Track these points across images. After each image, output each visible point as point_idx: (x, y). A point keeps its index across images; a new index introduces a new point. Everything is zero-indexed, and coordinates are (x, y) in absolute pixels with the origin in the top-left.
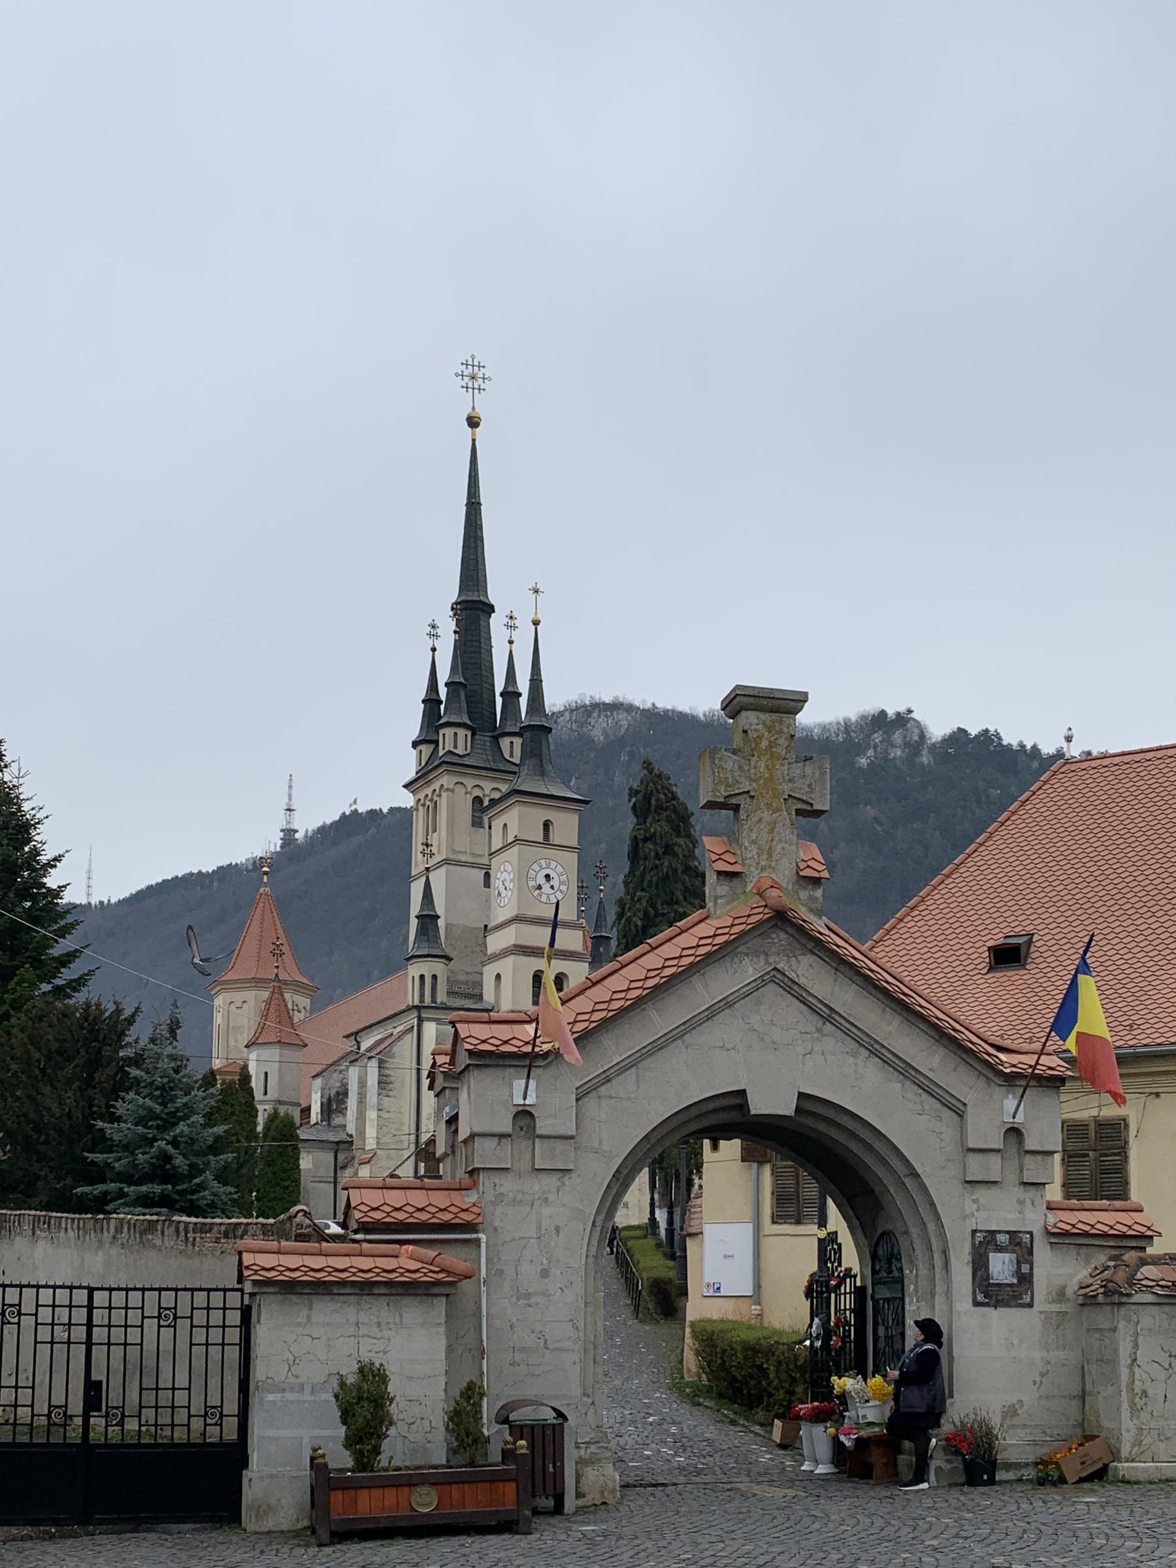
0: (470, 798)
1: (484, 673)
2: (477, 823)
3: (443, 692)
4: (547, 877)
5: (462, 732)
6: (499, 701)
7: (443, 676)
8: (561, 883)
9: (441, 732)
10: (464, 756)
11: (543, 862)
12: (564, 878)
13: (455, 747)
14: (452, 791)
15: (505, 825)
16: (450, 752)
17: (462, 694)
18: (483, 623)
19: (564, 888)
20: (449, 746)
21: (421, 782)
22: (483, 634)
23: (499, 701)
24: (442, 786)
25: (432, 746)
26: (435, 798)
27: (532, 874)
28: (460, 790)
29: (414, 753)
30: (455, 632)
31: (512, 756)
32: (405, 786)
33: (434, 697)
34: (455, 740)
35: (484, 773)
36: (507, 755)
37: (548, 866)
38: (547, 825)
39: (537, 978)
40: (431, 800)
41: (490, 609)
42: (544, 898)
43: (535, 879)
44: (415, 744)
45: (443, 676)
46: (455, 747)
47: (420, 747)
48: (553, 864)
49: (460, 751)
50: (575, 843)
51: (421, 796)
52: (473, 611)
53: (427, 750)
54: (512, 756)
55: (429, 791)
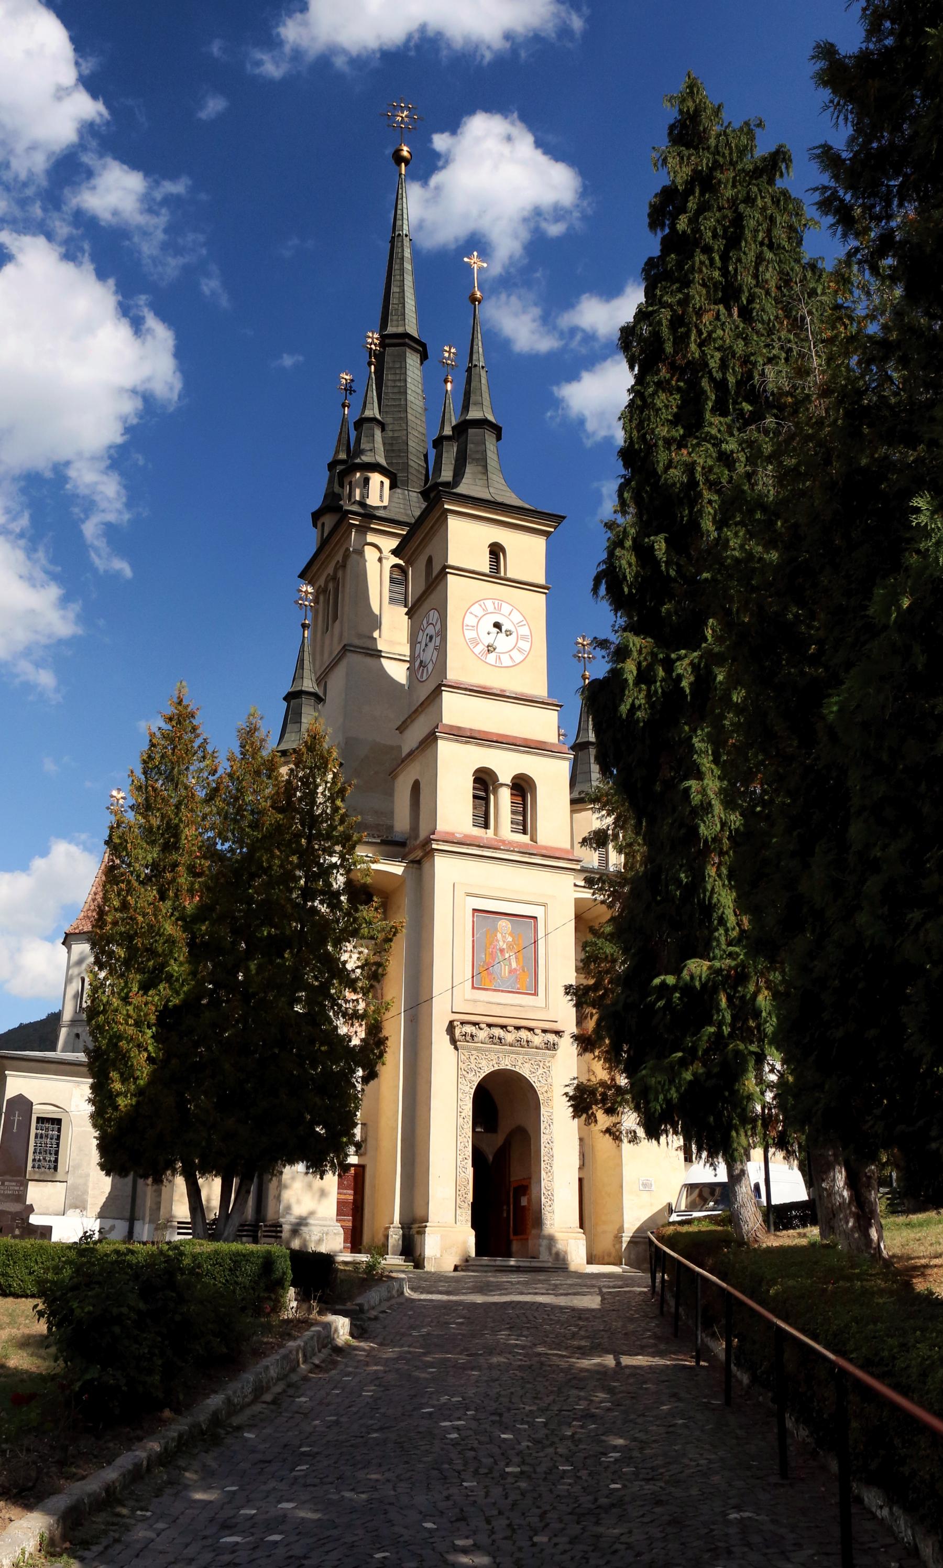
1: (410, 416)
4: (497, 625)
5: (376, 479)
10: (377, 508)
11: (489, 604)
15: (430, 561)
17: (378, 433)
18: (409, 361)
19: (525, 645)
21: (322, 557)
26: (340, 574)
27: (470, 620)
38: (496, 551)
39: (484, 781)
44: (316, 516)
47: (319, 525)
48: (506, 608)
50: (542, 580)
51: (321, 582)
53: (329, 521)
55: (330, 570)
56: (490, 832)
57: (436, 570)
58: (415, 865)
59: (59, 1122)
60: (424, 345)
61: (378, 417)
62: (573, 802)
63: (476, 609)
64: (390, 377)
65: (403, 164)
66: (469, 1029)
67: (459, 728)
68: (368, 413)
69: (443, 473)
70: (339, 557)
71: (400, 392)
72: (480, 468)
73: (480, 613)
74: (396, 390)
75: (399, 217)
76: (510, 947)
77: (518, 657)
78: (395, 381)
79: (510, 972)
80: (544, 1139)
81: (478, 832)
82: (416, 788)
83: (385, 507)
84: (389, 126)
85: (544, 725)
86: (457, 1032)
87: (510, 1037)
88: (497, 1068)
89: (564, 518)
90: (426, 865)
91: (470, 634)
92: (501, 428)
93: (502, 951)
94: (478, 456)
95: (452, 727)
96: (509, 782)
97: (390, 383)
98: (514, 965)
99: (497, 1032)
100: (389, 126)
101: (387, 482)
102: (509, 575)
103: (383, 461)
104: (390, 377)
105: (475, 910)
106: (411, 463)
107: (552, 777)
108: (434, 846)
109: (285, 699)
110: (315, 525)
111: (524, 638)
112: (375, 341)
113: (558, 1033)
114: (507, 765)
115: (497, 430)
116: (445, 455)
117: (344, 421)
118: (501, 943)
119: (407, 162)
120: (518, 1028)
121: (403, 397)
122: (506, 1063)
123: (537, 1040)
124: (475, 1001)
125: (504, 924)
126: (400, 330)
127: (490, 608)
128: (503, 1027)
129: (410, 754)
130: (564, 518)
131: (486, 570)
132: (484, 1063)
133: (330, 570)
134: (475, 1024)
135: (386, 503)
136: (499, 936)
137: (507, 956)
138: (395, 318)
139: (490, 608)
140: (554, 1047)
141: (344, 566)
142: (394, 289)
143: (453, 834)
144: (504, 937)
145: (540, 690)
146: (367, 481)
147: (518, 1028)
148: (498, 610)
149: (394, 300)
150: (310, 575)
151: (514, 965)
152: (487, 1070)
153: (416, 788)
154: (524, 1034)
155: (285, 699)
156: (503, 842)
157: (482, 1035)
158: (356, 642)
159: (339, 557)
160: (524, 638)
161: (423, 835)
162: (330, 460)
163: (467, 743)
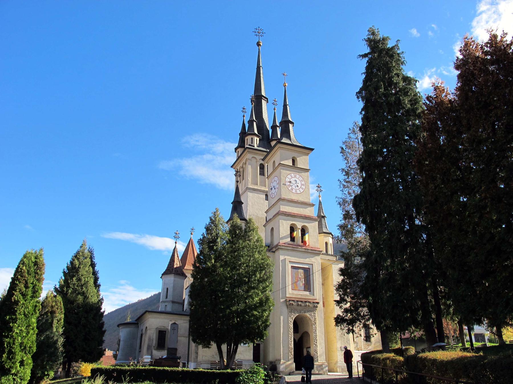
0: (259, 164)
3: (247, 126)
8: (302, 185)
12: (303, 183)
13: (252, 143)
14: (251, 160)
15: (274, 162)
19: (304, 187)
21: (238, 161)
26: (244, 166)
28: (254, 160)
29: (236, 154)
32: (232, 167)
37: (295, 177)
40: (242, 167)
42: (294, 191)
44: (236, 149)
45: (247, 119)
53: (240, 150)
56: (295, 243)
57: (276, 165)
59: (165, 331)
60: (267, 99)
73: (290, 177)
77: (302, 191)
81: (291, 243)
82: (272, 229)
86: (288, 303)
87: (303, 305)
90: (277, 253)
93: (300, 278)
95: (283, 212)
101: (258, 139)
102: (298, 166)
103: (257, 133)
105: (292, 266)
110: (236, 152)
111: (303, 185)
113: (318, 303)
115: (292, 123)
120: (306, 302)
123: (311, 305)
124: (293, 294)
125: (301, 271)
127: (293, 176)
129: (270, 220)
131: (291, 165)
133: (241, 165)
134: (293, 301)
139: (293, 176)
140: (317, 307)
141: (245, 164)
146: (252, 138)
148: (295, 177)
150: (234, 166)
153: (272, 229)
159: (244, 161)
160: (303, 185)
161: (275, 243)
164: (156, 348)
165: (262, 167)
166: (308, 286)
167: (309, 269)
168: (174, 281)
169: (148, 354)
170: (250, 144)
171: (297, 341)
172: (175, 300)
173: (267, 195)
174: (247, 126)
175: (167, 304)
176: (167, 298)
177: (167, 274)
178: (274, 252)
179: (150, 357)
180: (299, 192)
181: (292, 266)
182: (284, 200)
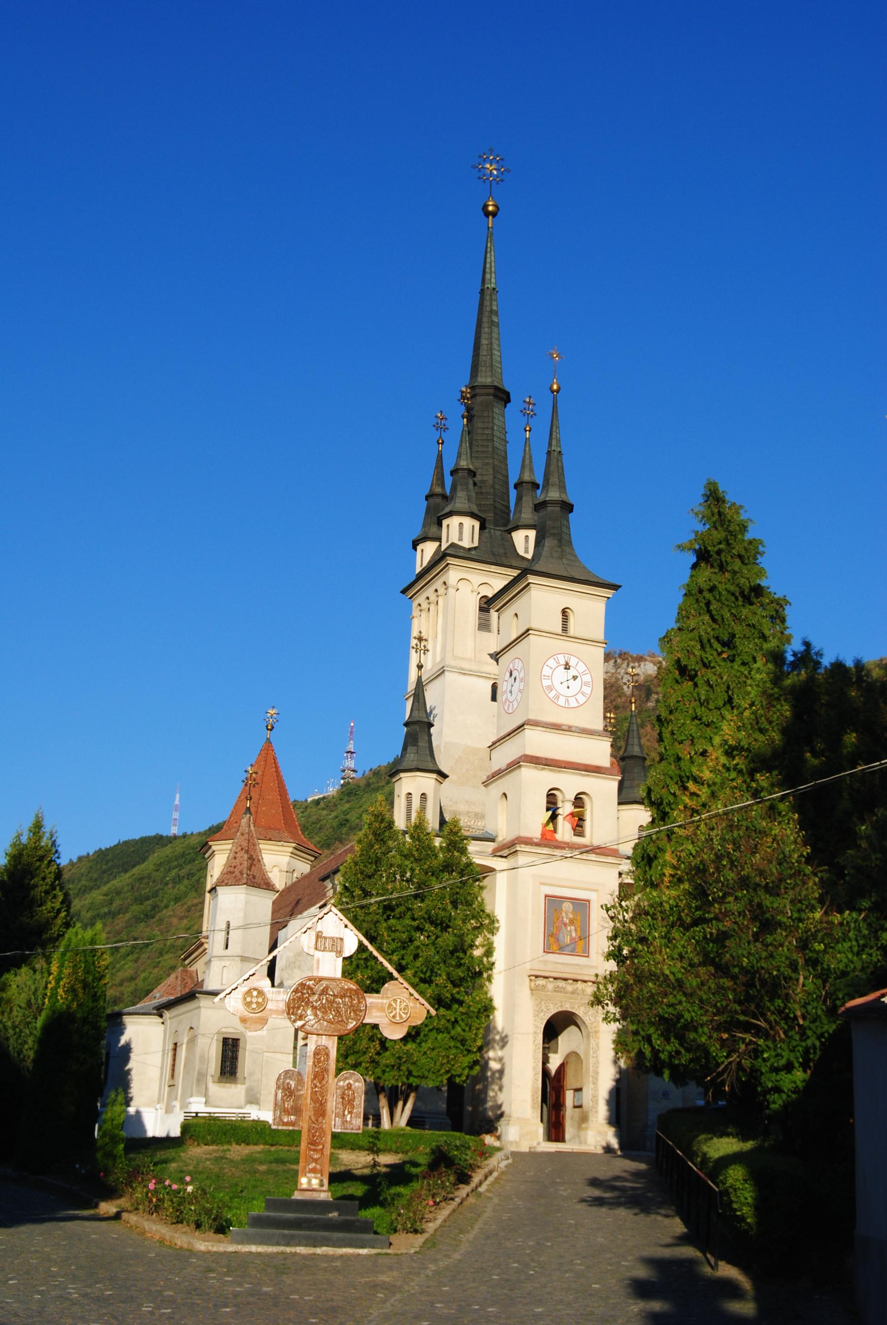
2: (484, 626)
3: (448, 480)
5: (470, 523)
6: (513, 494)
7: (448, 467)
9: (445, 523)
10: (470, 549)
13: (461, 539)
16: (453, 545)
18: (496, 410)
19: (587, 690)
20: (454, 539)
22: (496, 421)
23: (513, 494)
24: (445, 583)
25: (435, 545)
27: (546, 671)
30: (463, 417)
31: (527, 552)
33: (438, 490)
34: (461, 530)
35: (493, 568)
36: (521, 551)
41: (504, 397)
42: (562, 701)
43: (550, 677)
46: (461, 539)
47: (419, 548)
49: (466, 543)
52: (486, 399)
54: (527, 552)
58: (504, 859)
60: (508, 394)
61: (471, 467)
62: (620, 804)
63: (551, 663)
64: (480, 425)
65: (491, 218)
66: (541, 982)
67: (537, 758)
68: (464, 464)
69: (523, 516)
70: (438, 584)
71: (487, 440)
72: (556, 542)
74: (484, 437)
75: (488, 270)
76: (572, 922)
77: (582, 699)
78: (483, 429)
79: (571, 940)
80: (591, 1060)
83: (475, 548)
84: (479, 178)
85: (600, 751)
86: (533, 984)
88: (560, 1009)
89: (620, 587)
91: (546, 683)
92: (572, 506)
93: (565, 925)
94: (555, 531)
96: (573, 798)
97: (479, 431)
98: (574, 935)
99: (561, 984)
100: (479, 178)
101: (477, 525)
102: (577, 635)
103: (475, 509)
104: (480, 425)
105: (546, 896)
106: (497, 505)
107: (605, 789)
108: (518, 849)
109: (406, 724)
111: (586, 684)
112: (468, 395)
114: (569, 785)
116: (524, 499)
117: (440, 457)
118: (565, 919)
119: (494, 214)
120: (576, 981)
121: (490, 444)
122: (567, 1007)
124: (545, 962)
125: (567, 906)
126: (488, 381)
128: (565, 980)
130: (620, 587)
131: (560, 631)
132: (552, 1006)
135: (476, 544)
136: (564, 914)
137: (569, 928)
138: (484, 368)
142: (484, 342)
143: (532, 839)
144: (567, 915)
145: (599, 725)
147: (576, 981)
149: (483, 352)
151: (574, 935)
152: (553, 1011)
154: (580, 985)
155: (406, 724)
156: (567, 843)
157: (551, 985)
158: (453, 663)
160: (586, 684)
162: (427, 492)
163: (543, 769)
164: (216, 1079)
165: (486, 604)
166: (580, 945)
167: (589, 901)
168: (246, 903)
169: (199, 1094)
170: (456, 541)
171: (553, 1072)
172: (248, 954)
173: (494, 687)
174: (448, 480)
175: (227, 963)
176: (227, 948)
177: (226, 885)
178: (506, 857)
179: (204, 1100)
180: (573, 703)
181: (546, 896)
182: (536, 724)
